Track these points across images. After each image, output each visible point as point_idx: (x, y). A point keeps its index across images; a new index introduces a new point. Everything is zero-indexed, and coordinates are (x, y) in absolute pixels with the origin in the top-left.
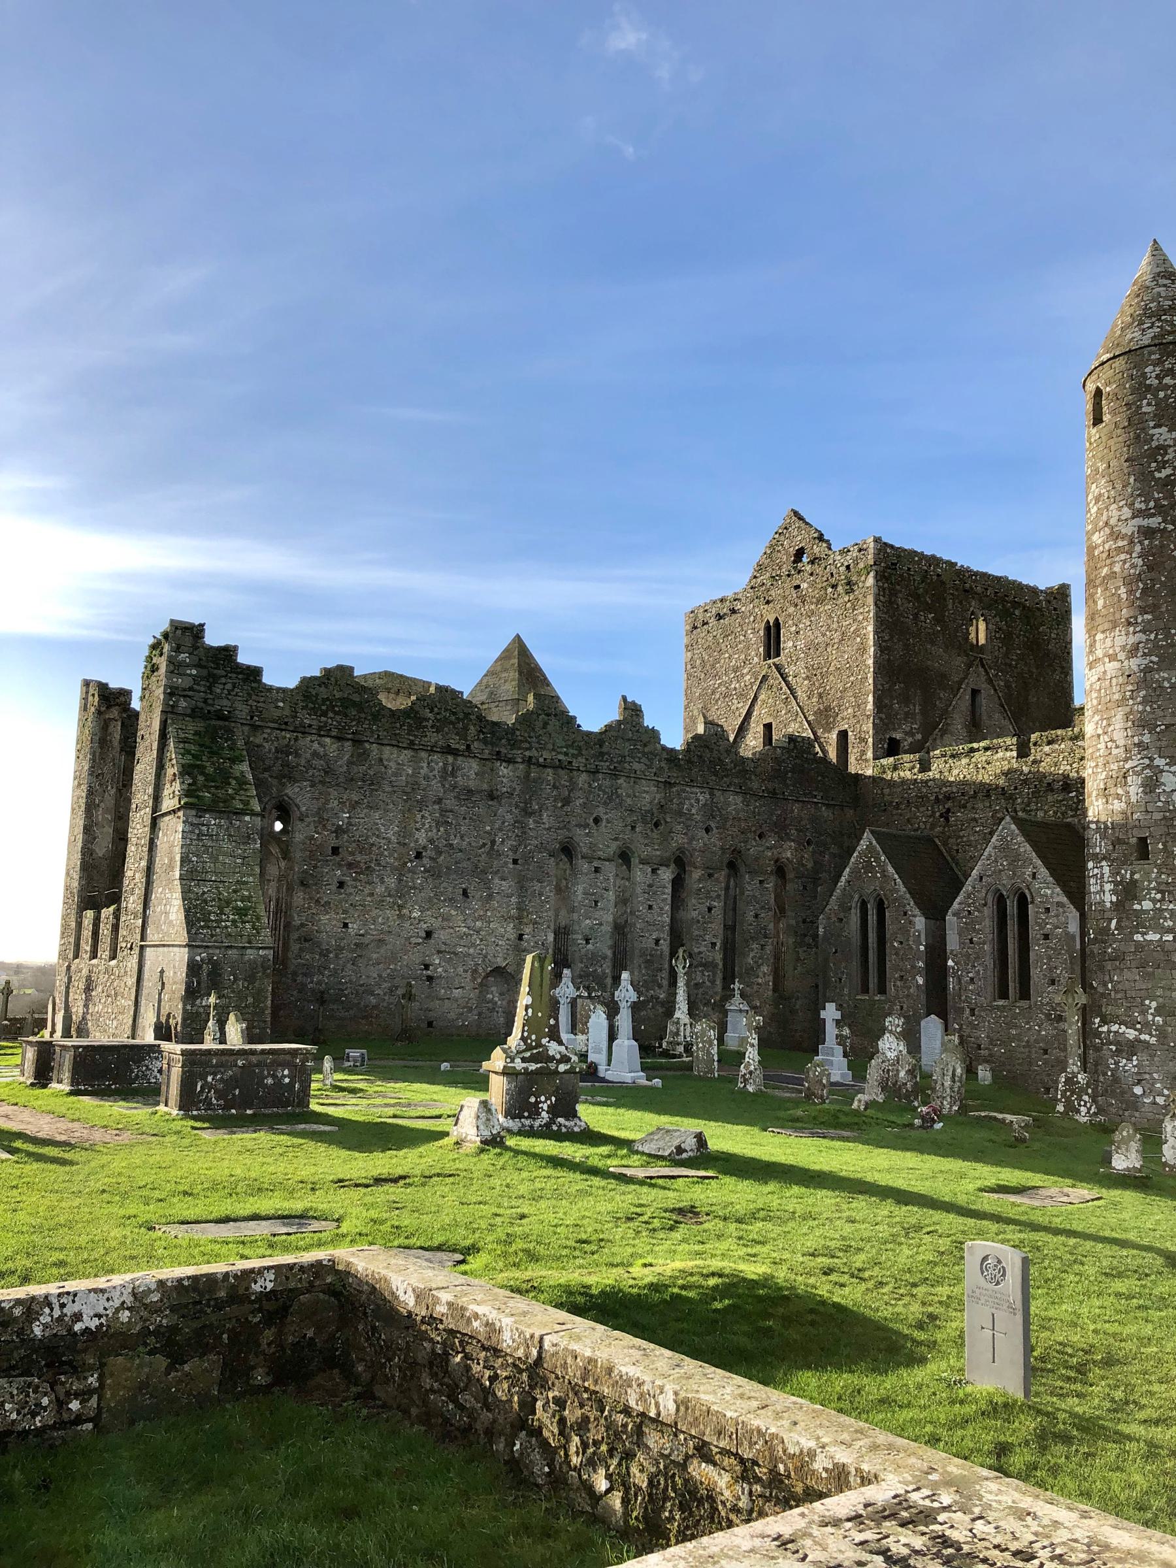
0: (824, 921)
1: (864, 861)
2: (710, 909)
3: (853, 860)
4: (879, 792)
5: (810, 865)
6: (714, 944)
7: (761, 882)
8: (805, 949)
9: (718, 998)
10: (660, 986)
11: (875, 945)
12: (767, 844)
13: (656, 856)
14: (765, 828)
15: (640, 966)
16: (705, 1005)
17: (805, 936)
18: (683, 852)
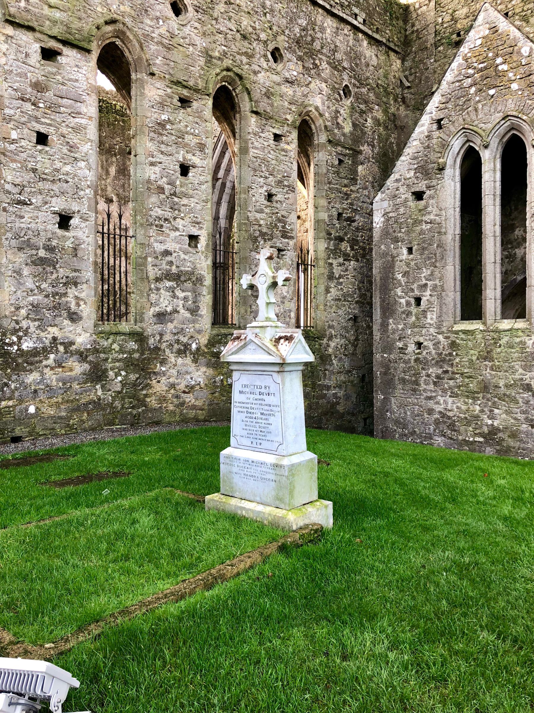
0: (385, 204)
1: (481, 70)
2: (185, 170)
3: (449, 77)
4: (448, 18)
5: (348, 128)
6: (193, 239)
7: (277, 138)
8: (341, 260)
9: (204, 340)
10: (74, 317)
11: (498, 229)
12: (287, 75)
13: (55, 22)
14: (282, 42)
15: (18, 272)
16: (181, 353)
17: (341, 239)
18: (120, 34)
